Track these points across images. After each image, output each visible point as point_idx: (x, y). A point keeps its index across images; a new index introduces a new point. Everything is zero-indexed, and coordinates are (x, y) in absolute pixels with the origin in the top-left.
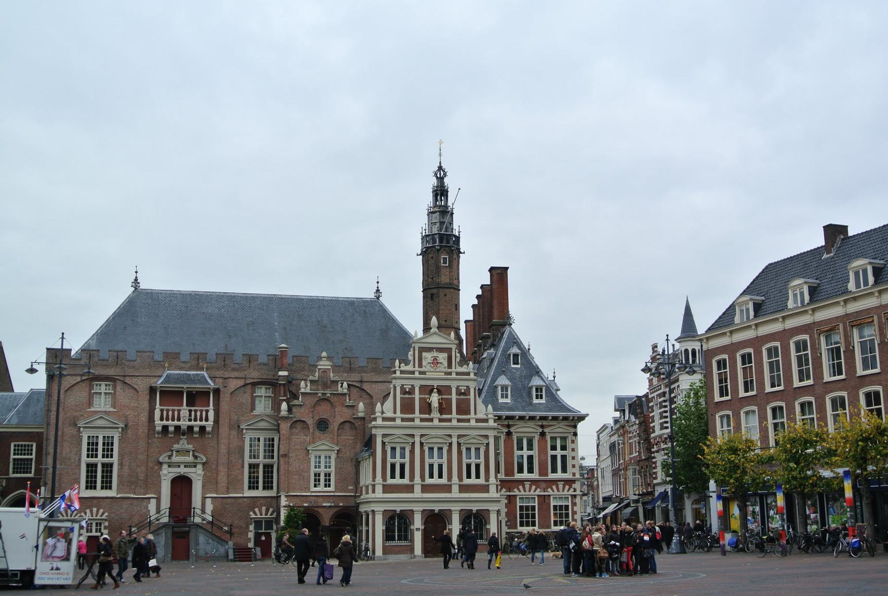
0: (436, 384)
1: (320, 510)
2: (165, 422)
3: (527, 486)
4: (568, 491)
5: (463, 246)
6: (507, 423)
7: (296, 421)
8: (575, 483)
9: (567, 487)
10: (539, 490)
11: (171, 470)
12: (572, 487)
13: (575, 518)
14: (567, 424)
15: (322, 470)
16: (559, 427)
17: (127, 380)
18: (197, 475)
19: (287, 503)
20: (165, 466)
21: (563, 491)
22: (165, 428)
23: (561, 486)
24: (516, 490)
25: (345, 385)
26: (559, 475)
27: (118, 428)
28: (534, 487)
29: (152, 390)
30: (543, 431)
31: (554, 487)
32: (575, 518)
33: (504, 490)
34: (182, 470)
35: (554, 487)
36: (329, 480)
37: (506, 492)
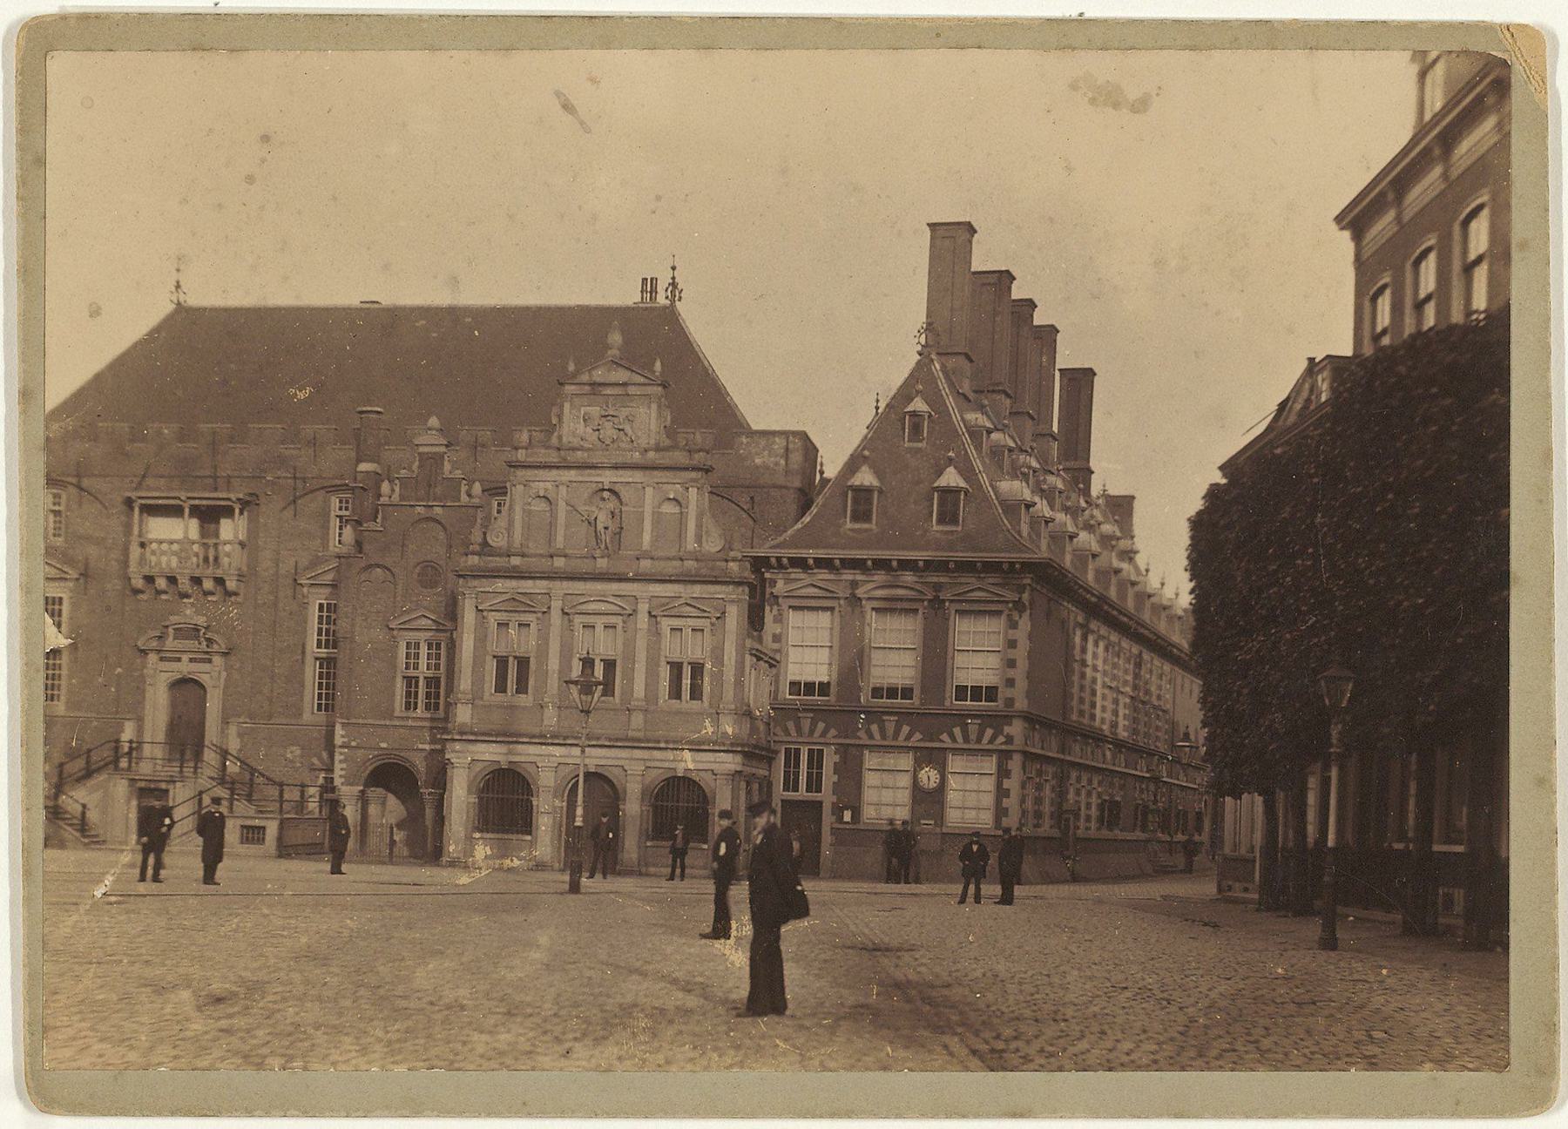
0: (607, 477)
6: (850, 577)
7: (370, 566)
8: (1010, 724)
9: (989, 732)
10: (918, 736)
12: (1001, 732)
13: (1004, 805)
14: (1000, 581)
17: (86, 483)
18: (212, 675)
19: (346, 740)
20: (152, 657)
21: (979, 741)
25: (477, 488)
28: (906, 729)
29: (129, 503)
32: (1004, 805)
33: (833, 732)
34: (185, 668)
35: (957, 731)
37: (834, 737)
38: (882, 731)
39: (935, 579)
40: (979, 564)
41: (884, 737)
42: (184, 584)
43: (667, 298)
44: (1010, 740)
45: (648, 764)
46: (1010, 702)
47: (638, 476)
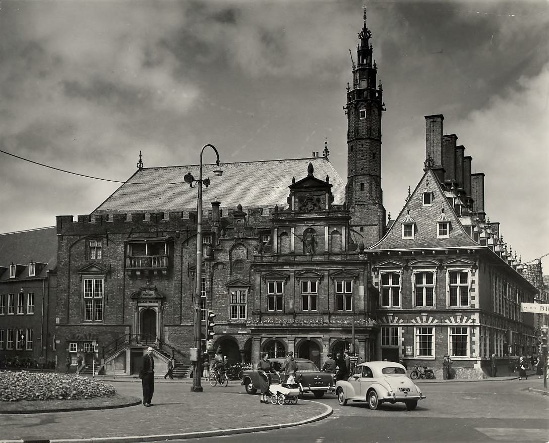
1: (237, 337)
2: (133, 268)
3: (424, 318)
4: (466, 322)
5: (384, 100)
10: (436, 321)
11: (139, 305)
14: (466, 257)
15: (238, 304)
16: (458, 261)
22: (134, 272)
23: (459, 318)
24: (413, 321)
26: (459, 306)
27: (103, 274)
30: (441, 265)
31: (452, 318)
33: (401, 321)
34: (148, 304)
35: (452, 318)
36: (244, 312)
38: (421, 319)
39: (439, 258)
40: (458, 251)
41: (422, 322)
42: (147, 273)
43: (324, 155)
44: (474, 321)
45: (331, 336)
46: (472, 306)
47: (322, 223)
